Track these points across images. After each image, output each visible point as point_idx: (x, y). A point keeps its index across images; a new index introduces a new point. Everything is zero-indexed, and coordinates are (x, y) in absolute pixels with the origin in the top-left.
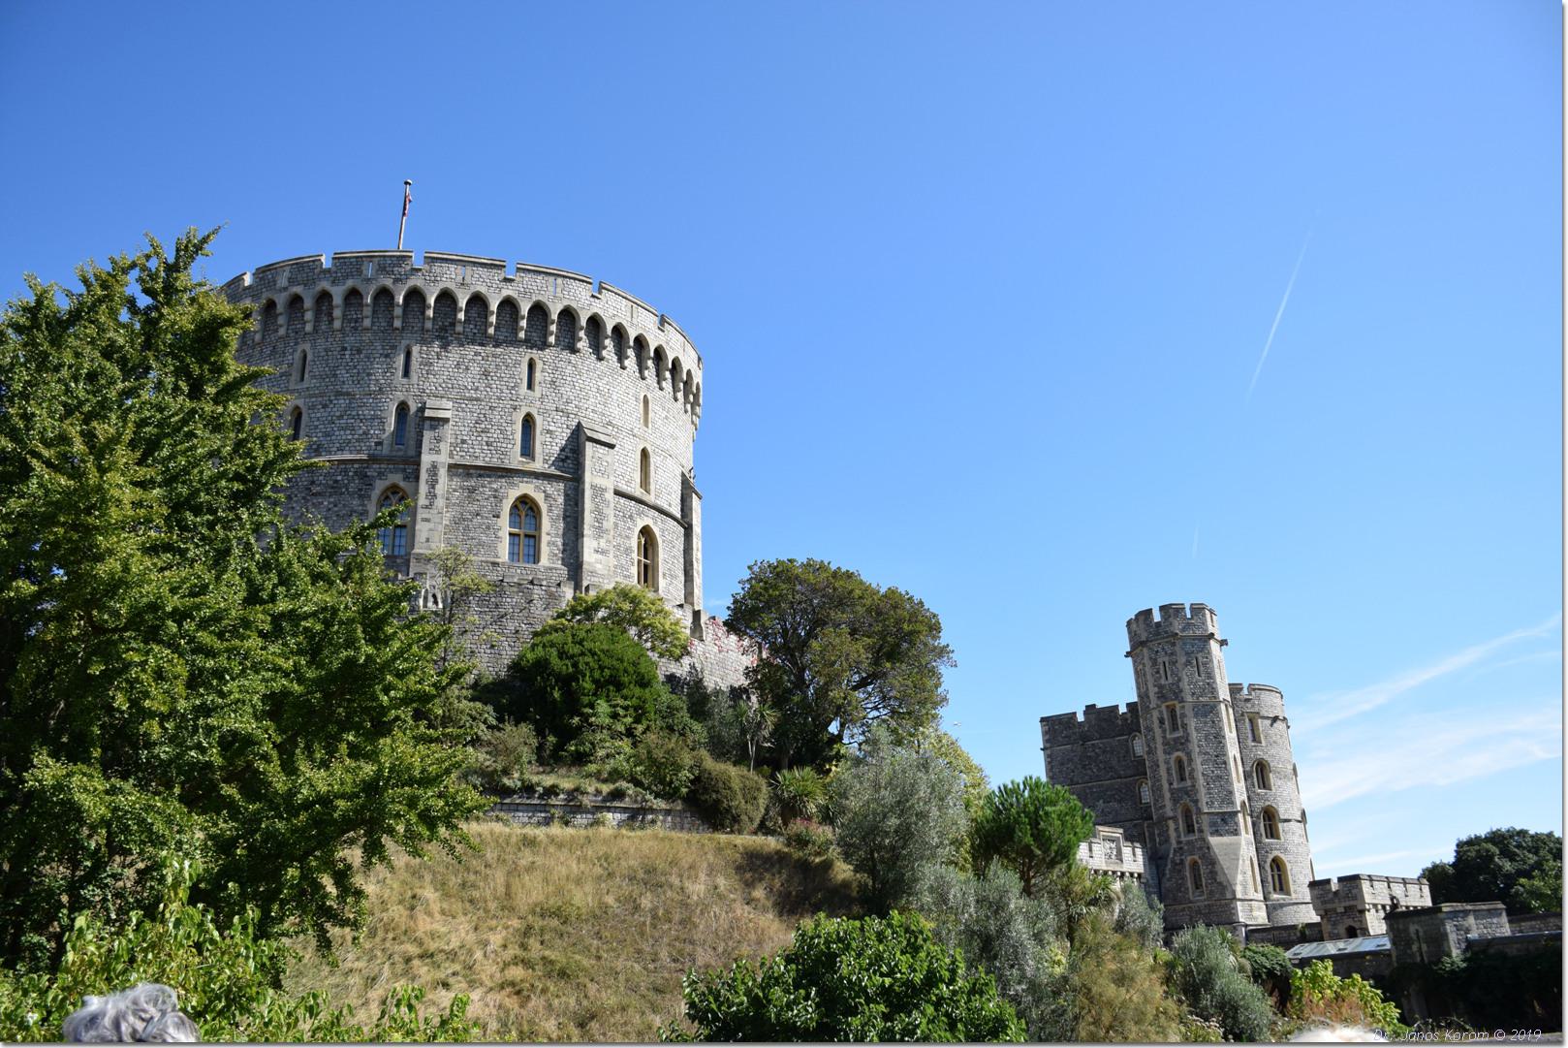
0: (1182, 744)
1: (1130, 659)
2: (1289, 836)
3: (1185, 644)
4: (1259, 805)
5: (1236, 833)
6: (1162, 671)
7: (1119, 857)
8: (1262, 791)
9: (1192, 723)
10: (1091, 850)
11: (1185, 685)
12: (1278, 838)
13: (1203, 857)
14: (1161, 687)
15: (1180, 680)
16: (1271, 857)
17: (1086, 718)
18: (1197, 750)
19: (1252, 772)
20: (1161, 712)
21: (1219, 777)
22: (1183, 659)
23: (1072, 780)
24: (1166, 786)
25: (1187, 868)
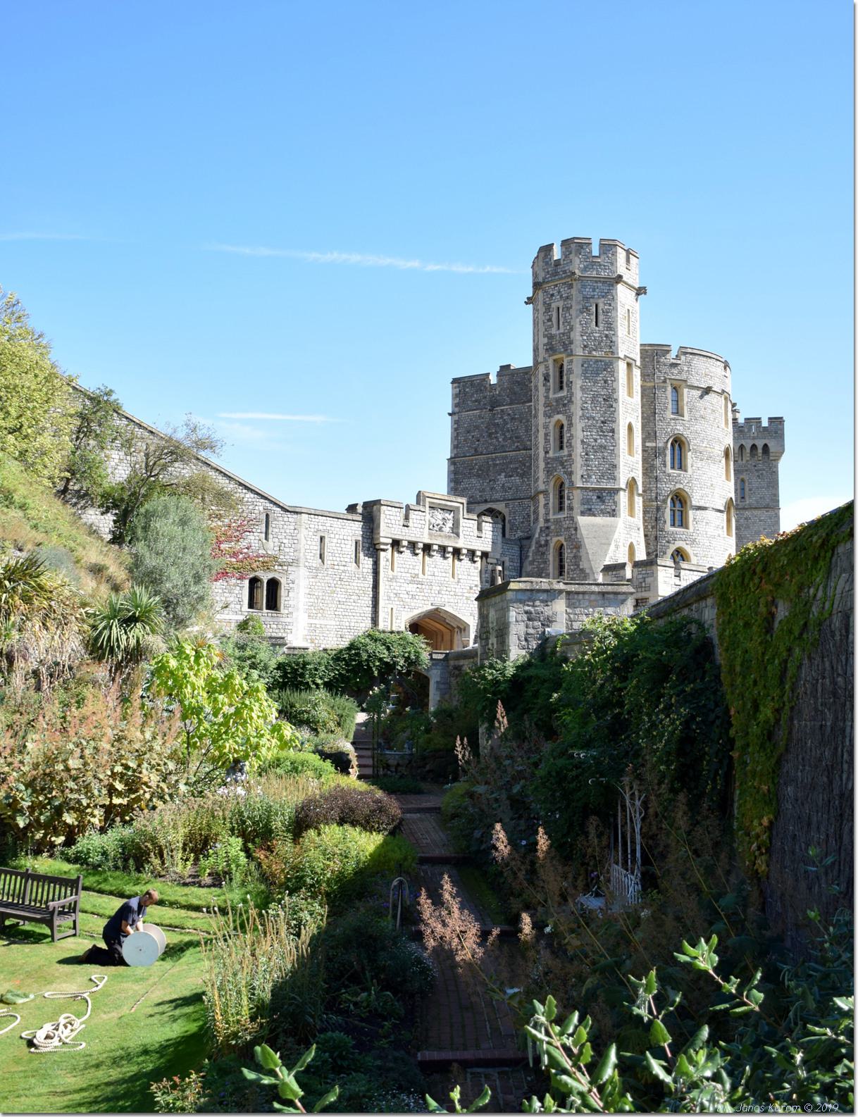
0: (564, 405)
1: (531, 306)
2: (701, 527)
3: (584, 286)
4: (667, 488)
5: (613, 513)
6: (554, 319)
7: (455, 530)
8: (676, 472)
9: (578, 383)
10: (407, 518)
11: (576, 336)
12: (687, 528)
13: (569, 539)
14: (551, 337)
15: (571, 329)
16: (672, 548)
17: (499, 381)
18: (580, 413)
19: (665, 448)
20: (547, 367)
21: (603, 447)
22: (576, 307)
23: (476, 450)
24: (542, 454)
25: (551, 551)
